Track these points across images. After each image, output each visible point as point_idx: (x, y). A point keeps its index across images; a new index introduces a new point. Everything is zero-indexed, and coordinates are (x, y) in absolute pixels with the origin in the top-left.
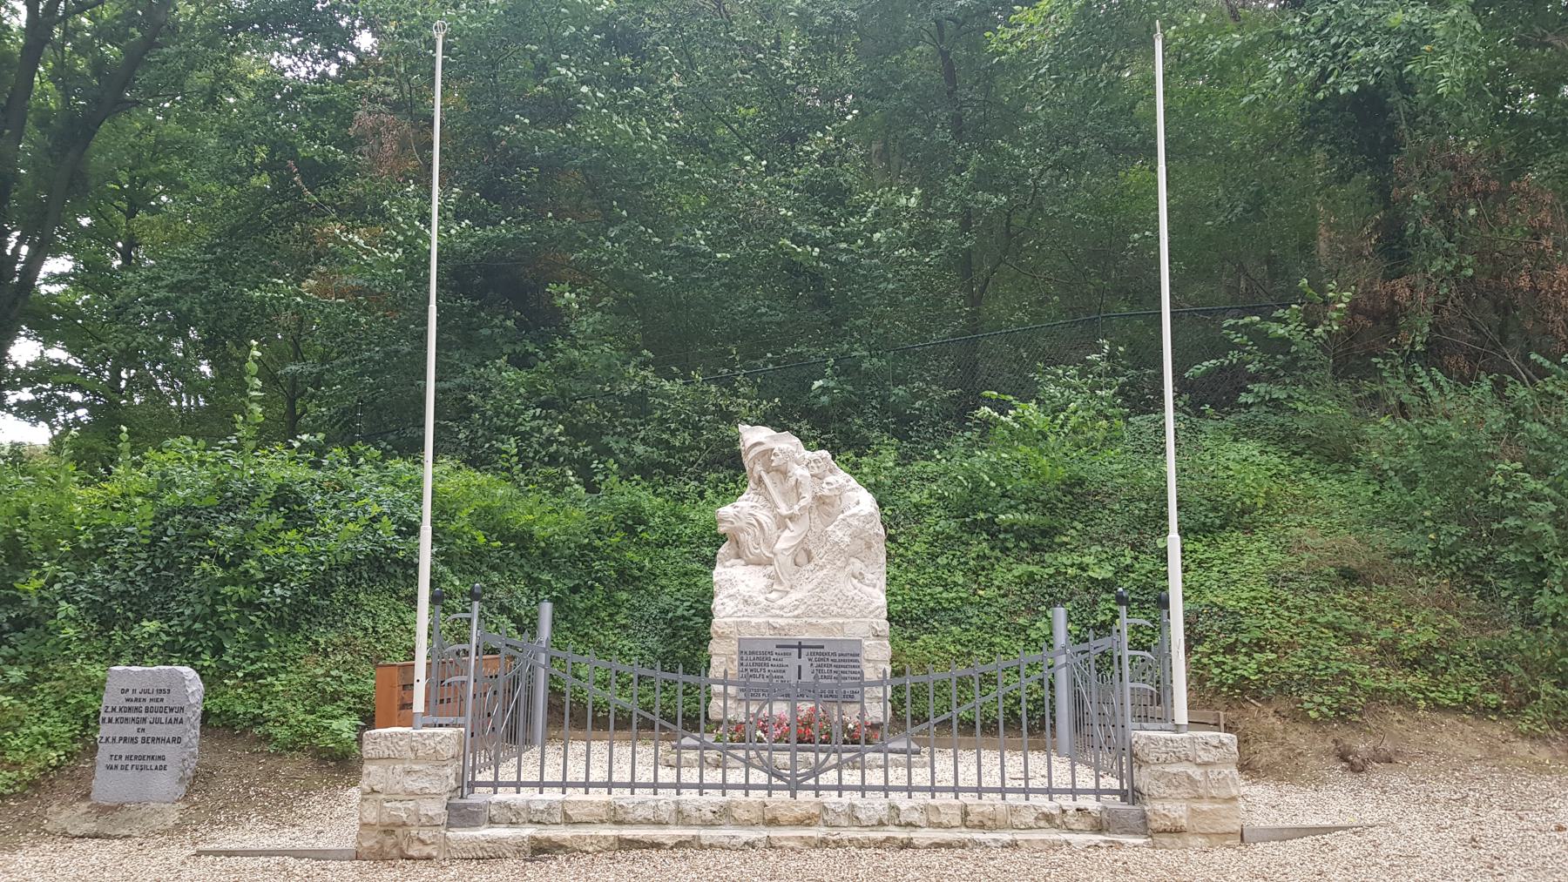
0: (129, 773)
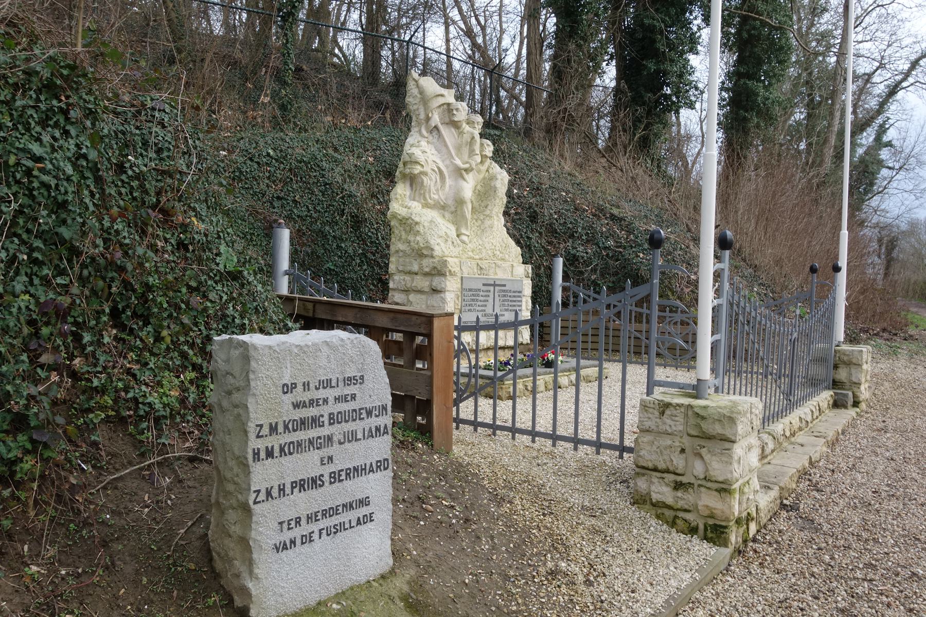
0: (318, 544)
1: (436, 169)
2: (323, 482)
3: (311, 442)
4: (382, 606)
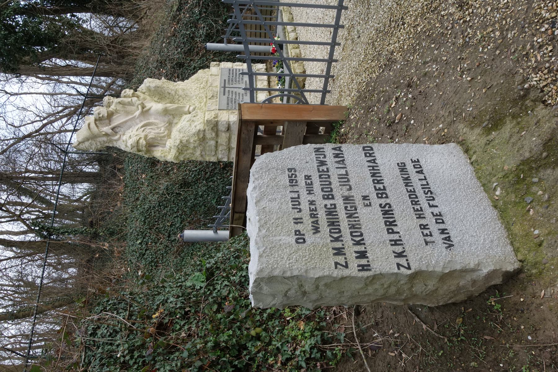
0: (443, 208)
1: (142, 129)
2: (386, 204)
3: (350, 216)
4: (496, 150)
